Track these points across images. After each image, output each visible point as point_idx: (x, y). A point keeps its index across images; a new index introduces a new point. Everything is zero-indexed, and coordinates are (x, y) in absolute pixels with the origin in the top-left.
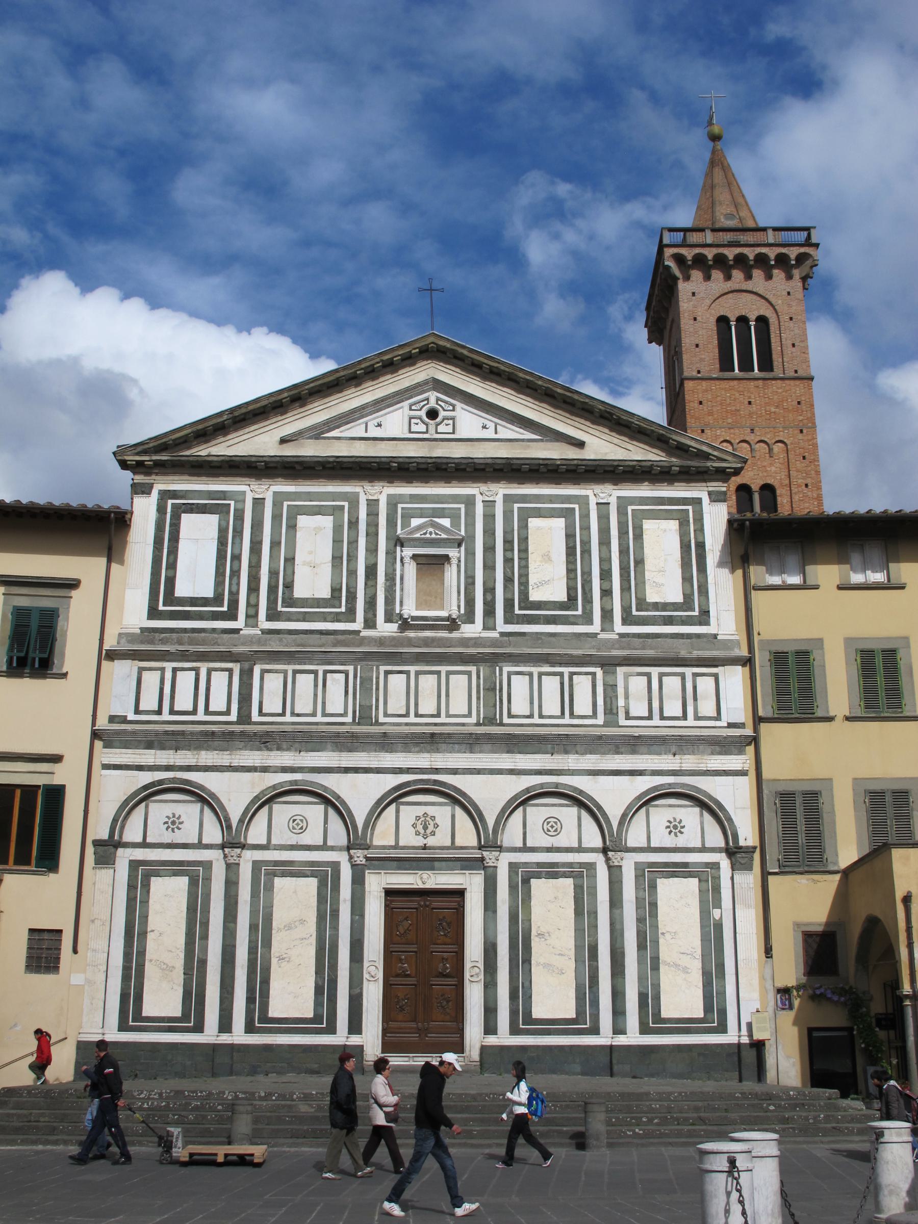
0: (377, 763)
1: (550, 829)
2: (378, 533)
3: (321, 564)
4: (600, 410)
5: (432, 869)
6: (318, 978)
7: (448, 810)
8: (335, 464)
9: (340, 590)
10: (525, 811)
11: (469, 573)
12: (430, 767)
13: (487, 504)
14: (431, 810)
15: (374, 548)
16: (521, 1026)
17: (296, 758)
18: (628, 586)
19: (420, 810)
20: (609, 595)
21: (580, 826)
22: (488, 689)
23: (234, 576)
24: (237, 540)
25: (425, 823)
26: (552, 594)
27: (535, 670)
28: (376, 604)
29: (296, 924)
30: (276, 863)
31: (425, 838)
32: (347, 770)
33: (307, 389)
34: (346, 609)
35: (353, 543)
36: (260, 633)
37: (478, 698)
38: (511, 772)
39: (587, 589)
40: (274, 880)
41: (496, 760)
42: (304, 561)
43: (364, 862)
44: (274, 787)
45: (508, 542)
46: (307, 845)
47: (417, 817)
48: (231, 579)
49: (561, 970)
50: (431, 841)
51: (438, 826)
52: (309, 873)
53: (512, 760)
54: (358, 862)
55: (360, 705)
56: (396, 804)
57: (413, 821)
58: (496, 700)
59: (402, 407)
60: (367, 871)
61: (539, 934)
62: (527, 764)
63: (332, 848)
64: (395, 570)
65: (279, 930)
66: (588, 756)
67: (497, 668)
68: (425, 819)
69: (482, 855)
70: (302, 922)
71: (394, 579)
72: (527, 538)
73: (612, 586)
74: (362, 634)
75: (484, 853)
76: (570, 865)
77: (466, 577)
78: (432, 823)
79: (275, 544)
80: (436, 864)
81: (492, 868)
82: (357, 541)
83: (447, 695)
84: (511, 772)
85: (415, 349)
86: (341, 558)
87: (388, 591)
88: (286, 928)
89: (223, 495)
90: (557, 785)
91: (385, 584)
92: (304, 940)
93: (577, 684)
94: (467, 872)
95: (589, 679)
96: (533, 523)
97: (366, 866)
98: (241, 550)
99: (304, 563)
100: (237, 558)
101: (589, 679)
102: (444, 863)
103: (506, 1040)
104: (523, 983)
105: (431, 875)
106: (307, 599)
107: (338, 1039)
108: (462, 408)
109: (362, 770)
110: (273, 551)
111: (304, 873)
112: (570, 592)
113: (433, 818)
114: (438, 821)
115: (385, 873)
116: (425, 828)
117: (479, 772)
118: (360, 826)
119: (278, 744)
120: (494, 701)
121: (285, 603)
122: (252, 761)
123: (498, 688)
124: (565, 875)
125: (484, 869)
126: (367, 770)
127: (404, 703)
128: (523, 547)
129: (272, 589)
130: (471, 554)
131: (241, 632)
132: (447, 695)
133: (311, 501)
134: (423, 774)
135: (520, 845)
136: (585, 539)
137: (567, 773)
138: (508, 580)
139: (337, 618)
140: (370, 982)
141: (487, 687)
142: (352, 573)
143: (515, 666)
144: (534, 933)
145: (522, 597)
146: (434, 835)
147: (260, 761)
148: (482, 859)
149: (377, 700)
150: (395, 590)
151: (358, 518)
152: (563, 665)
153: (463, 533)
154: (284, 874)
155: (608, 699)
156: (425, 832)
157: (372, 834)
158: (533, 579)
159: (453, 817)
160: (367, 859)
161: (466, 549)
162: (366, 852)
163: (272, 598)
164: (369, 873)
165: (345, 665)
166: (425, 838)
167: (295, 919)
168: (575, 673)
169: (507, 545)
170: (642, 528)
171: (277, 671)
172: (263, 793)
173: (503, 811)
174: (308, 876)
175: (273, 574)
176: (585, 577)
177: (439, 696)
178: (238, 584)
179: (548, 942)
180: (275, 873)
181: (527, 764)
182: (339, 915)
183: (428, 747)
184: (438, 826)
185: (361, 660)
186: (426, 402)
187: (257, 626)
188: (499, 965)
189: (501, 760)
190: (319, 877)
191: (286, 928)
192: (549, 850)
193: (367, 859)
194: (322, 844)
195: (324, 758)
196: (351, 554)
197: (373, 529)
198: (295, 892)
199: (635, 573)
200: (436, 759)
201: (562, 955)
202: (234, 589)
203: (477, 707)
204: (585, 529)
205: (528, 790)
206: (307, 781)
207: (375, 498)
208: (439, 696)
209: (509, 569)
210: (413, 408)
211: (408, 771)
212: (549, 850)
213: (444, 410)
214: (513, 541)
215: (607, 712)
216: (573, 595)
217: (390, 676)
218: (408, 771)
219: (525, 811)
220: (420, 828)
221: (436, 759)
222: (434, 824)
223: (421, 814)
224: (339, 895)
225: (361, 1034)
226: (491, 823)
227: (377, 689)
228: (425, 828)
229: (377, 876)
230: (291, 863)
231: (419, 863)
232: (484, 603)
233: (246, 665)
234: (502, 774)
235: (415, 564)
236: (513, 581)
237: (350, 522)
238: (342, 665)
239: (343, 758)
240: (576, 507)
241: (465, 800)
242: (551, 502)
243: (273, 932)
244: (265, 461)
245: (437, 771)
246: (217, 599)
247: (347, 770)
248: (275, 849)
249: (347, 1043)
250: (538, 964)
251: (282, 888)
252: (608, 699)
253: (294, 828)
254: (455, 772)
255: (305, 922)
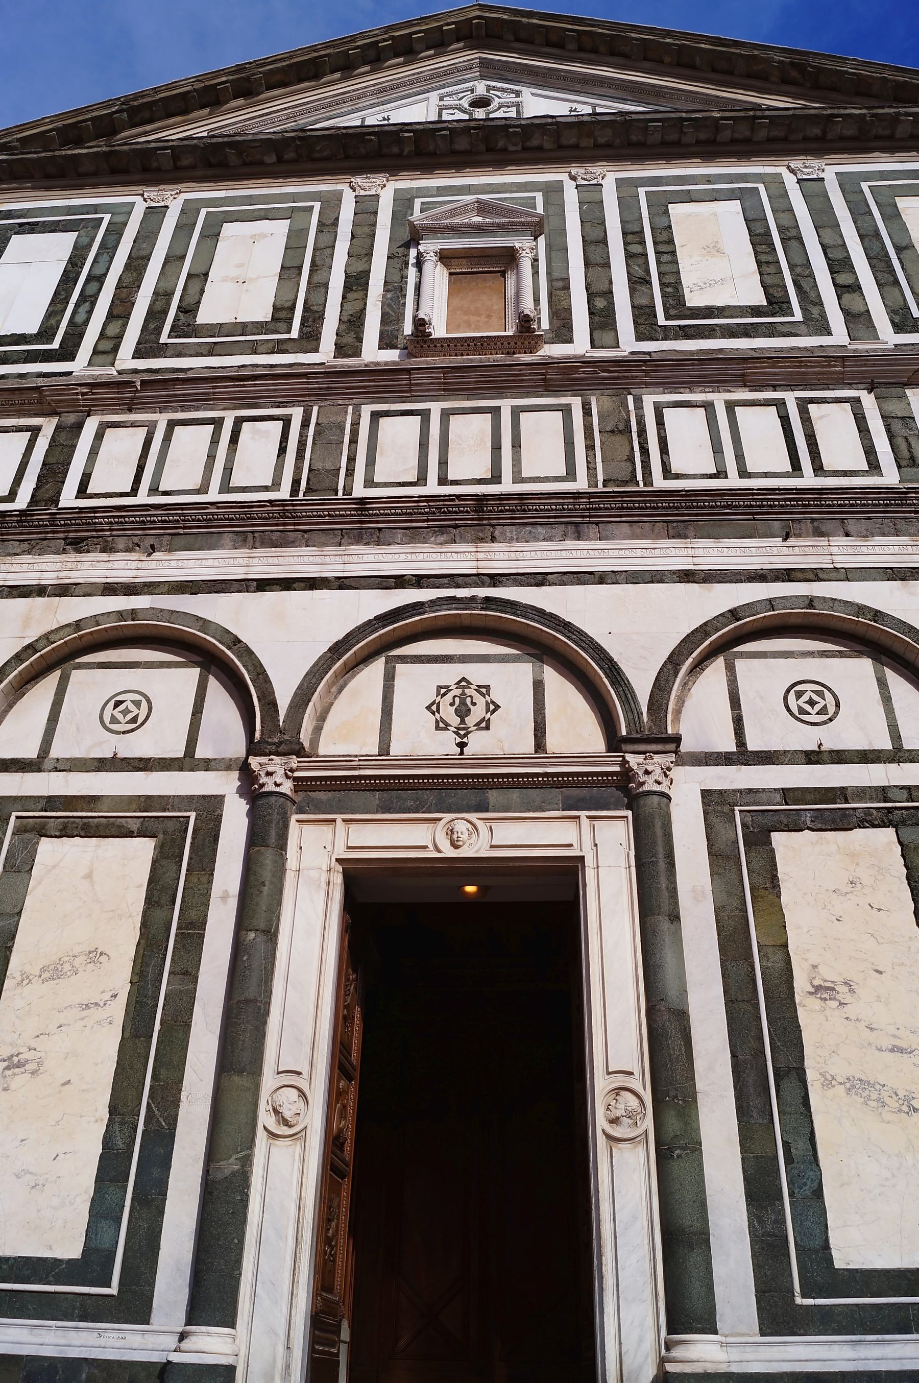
0: (340, 567)
1: (807, 708)
2: (374, 234)
3: (257, 278)
4: (780, 62)
5: (481, 807)
6: (117, 1127)
7: (524, 671)
8: (298, 142)
9: (292, 308)
10: (730, 669)
11: (556, 275)
12: (474, 572)
13: (585, 189)
14: (477, 673)
15: (364, 252)
16: (799, 1300)
17: (140, 565)
18: (891, 279)
19: (449, 674)
20: (854, 291)
21: (887, 699)
22: (612, 432)
23: (85, 301)
24: (105, 257)
25: (463, 702)
26: (733, 297)
27: (719, 399)
28: (363, 324)
29: (77, 963)
30: (51, 802)
31: (462, 737)
32: (263, 585)
33: (260, 73)
34: (300, 335)
35: (324, 252)
36: (115, 373)
37: (590, 447)
38: (687, 576)
39: (806, 286)
40: (38, 843)
41: (646, 553)
42: (226, 277)
43: (287, 787)
44: (78, 625)
45: (632, 235)
46: (141, 759)
47: (439, 688)
48: (77, 306)
49: (908, 1099)
50: (478, 744)
51: (497, 707)
52: (134, 826)
53: (685, 552)
54: (270, 787)
55: (310, 470)
56: (386, 663)
57: (432, 696)
58: (632, 448)
59: (427, 99)
60: (294, 817)
61: (818, 988)
62: (726, 560)
63: (207, 765)
64: (404, 278)
65: (26, 979)
66: (879, 540)
67: (630, 399)
68: (463, 693)
69: (624, 762)
70: (96, 956)
71: (401, 291)
72: (670, 227)
73: (857, 278)
74: (326, 364)
75: (629, 757)
76: (883, 793)
77: (551, 280)
78: (481, 701)
79: (174, 259)
80: (493, 796)
81: (656, 799)
82: (333, 247)
83: (516, 445)
84: (687, 576)
85: (448, 24)
86: (300, 268)
87: (389, 305)
88: (46, 975)
89: (95, 209)
90: (811, 602)
91: (384, 296)
92: (93, 1010)
93: (821, 418)
94: (583, 814)
95: (845, 410)
96: (676, 211)
97: (294, 802)
98: (108, 269)
99: (225, 279)
100: (96, 279)
101: (845, 410)
102: (515, 795)
103: (749, 1354)
104: (786, 1144)
105: (479, 824)
106: (221, 324)
107: (152, 1341)
108: (532, 94)
109: (303, 585)
110: (167, 267)
111: (120, 827)
112: (771, 291)
113: (484, 689)
114: (495, 696)
115: (344, 821)
116: (463, 712)
117: (601, 578)
118: (283, 701)
119: (106, 541)
120: (628, 448)
121: (175, 332)
122: (38, 575)
123: (634, 428)
124: (867, 821)
125: (629, 807)
126: (312, 584)
127: (414, 462)
128: (663, 237)
129: (155, 315)
130: (558, 249)
131: (73, 374)
132: (516, 445)
133: (251, 205)
134: (458, 586)
135: (729, 745)
136: (786, 223)
137: (834, 575)
138: (639, 282)
139: (279, 347)
140: (280, 1143)
141: (608, 428)
142: (319, 287)
143: (671, 393)
144: (801, 984)
145: (671, 302)
146: (487, 728)
147: (55, 575)
148: (627, 774)
149: (352, 459)
150: (404, 304)
151: (337, 219)
152: (777, 388)
153: (540, 210)
154: (66, 831)
155: (900, 441)
156: (463, 721)
157: (318, 730)
158: (687, 280)
159: (538, 686)
160: (301, 784)
161: (549, 247)
162: (294, 761)
163: (151, 326)
164: (298, 821)
165: (286, 407)
166: (462, 737)
167: (75, 952)
168: (812, 401)
169: (630, 238)
170: (897, 207)
171: (133, 425)
172: (47, 638)
173: (674, 661)
174: (130, 834)
175: (162, 296)
176: (798, 270)
177: (496, 448)
178: (90, 312)
179: (849, 1010)
180: (43, 826)
181: (726, 560)
182: (202, 936)
183: (470, 533)
184: (497, 707)
185: (319, 395)
186: (470, 92)
187: (113, 365)
188: (699, 1086)
189: (657, 552)
190: (161, 836)
191: (46, 975)
192: (813, 757)
193: (301, 784)
194: (181, 755)
195: (210, 562)
196: (318, 262)
197: (367, 230)
198: (89, 876)
199: (901, 262)
200: (493, 556)
201: (901, 1051)
202: (80, 318)
203: (588, 462)
204: (783, 212)
205: (734, 614)
206: (162, 610)
207: (372, 192)
208: (496, 448)
209: (638, 266)
210: (445, 99)
211: (419, 581)
212: (813, 757)
213: (499, 98)
214: (642, 231)
215: (903, 463)
216: (777, 293)
217: (383, 421)
218: (419, 581)
219: (730, 669)
220: (449, 714)
221: (493, 556)
222: (487, 704)
223: (451, 681)
224: (210, 882)
225: (233, 1325)
226: (643, 689)
227: (354, 441)
228: (463, 712)
229: (327, 829)
230: (91, 801)
231: (444, 793)
232: (591, 313)
233: (71, 418)
234: (661, 581)
235: (446, 273)
236: (649, 283)
237: (321, 224)
238: (278, 407)
239: (255, 561)
240: (761, 187)
241: (568, 637)
242: (709, 182)
243: (7, 984)
244: (171, 147)
245: (495, 580)
246: (46, 333)
247: (263, 585)
248: (56, 770)
249: (176, 1358)
250: (828, 1082)
251: (54, 867)
252: (900, 441)
253: (114, 720)
254: (540, 580)
255: (103, 959)
